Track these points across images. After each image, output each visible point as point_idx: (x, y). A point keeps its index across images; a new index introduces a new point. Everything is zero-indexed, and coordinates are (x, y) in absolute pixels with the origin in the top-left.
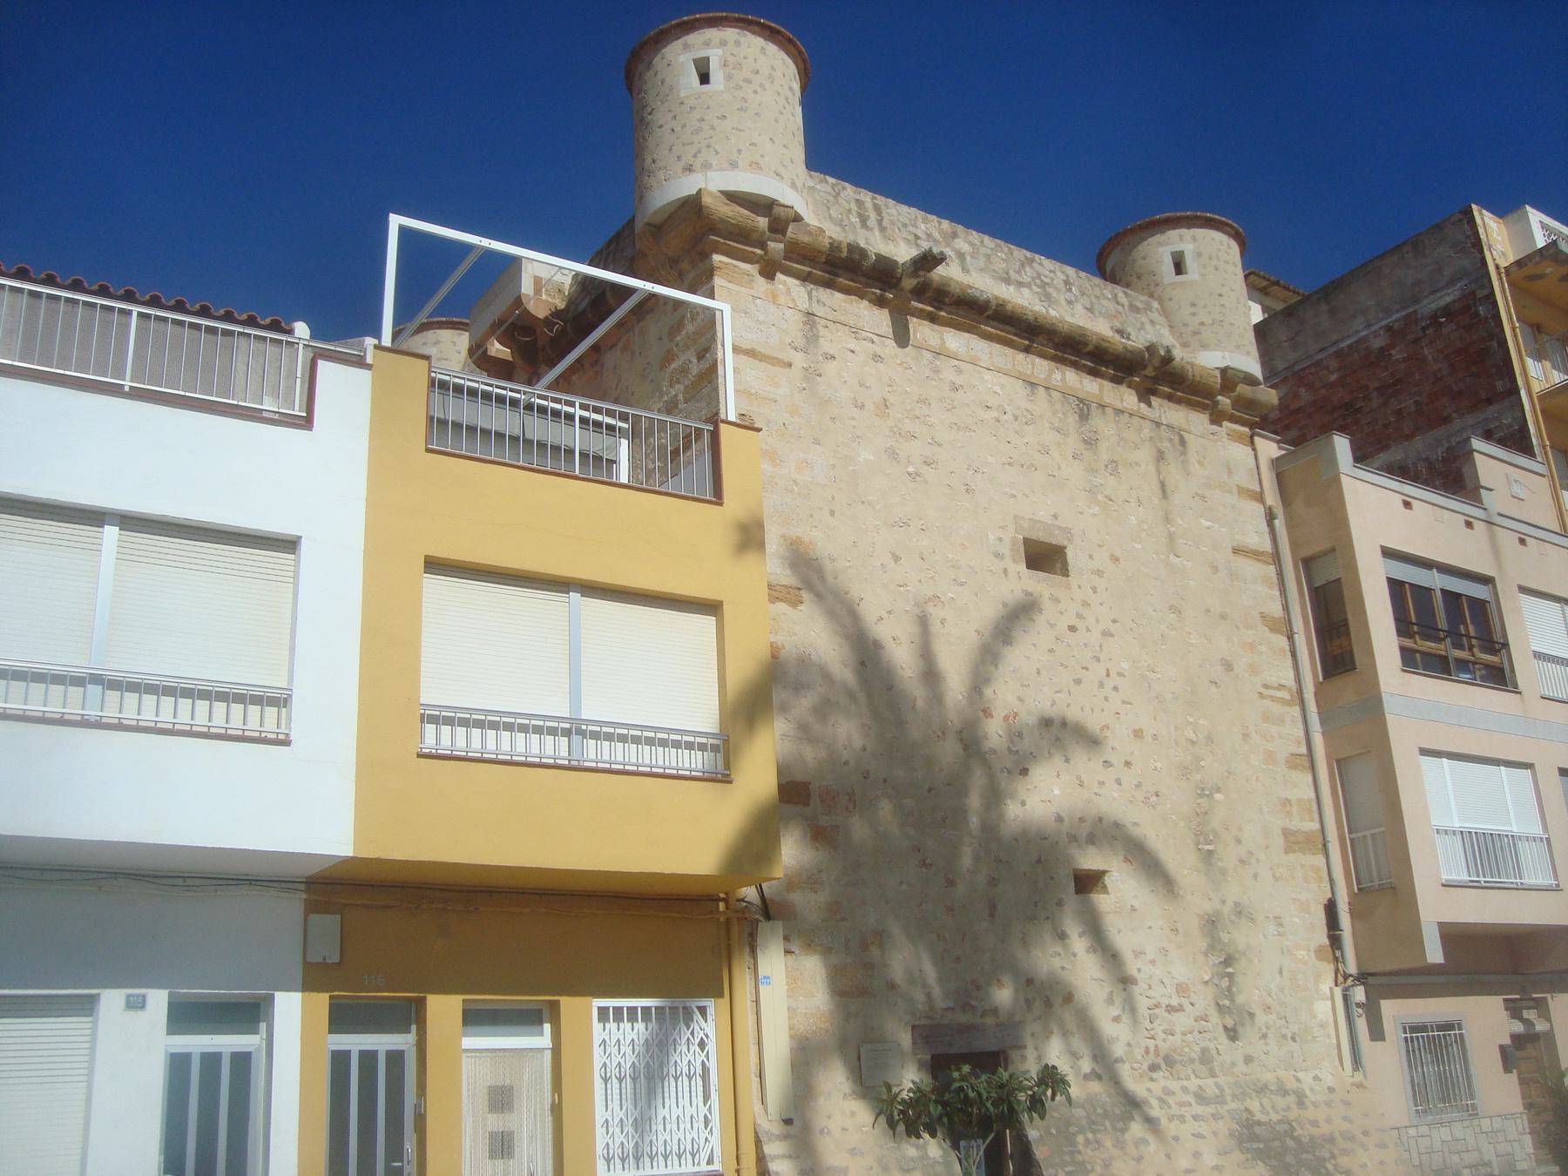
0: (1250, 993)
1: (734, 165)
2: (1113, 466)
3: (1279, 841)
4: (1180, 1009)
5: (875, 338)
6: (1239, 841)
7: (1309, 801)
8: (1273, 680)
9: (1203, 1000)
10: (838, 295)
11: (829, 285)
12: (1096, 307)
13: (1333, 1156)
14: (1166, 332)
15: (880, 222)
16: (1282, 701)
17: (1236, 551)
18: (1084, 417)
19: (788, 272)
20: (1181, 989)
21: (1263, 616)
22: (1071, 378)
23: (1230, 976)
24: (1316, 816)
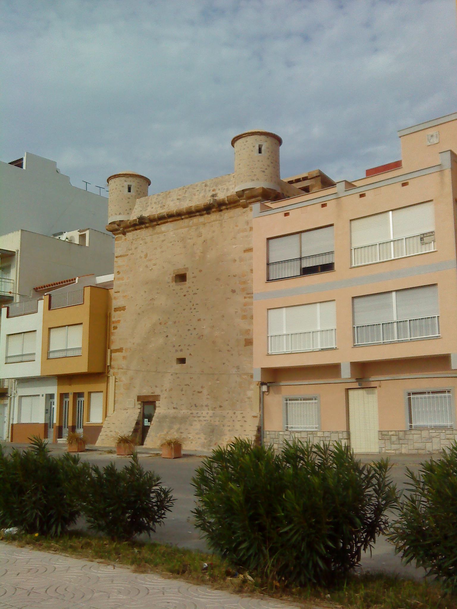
17: (245, 251)
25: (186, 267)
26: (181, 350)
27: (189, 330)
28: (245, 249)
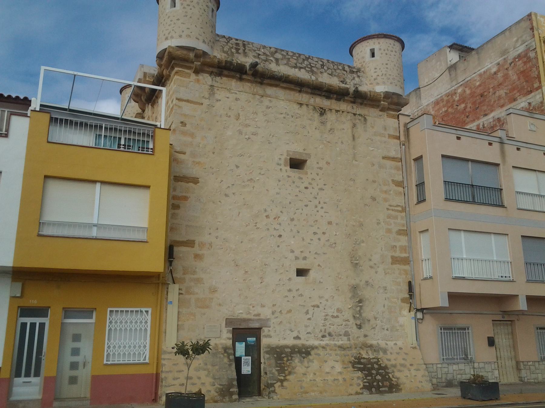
0: (367, 313)
4: (337, 317)
5: (237, 92)
6: (370, 260)
7: (405, 246)
8: (394, 203)
9: (348, 314)
12: (334, 73)
13: (393, 372)
15: (244, 50)
16: (398, 211)
17: (384, 158)
18: (322, 114)
20: (338, 310)
21: (393, 181)
23: (361, 307)
27: (315, 233)
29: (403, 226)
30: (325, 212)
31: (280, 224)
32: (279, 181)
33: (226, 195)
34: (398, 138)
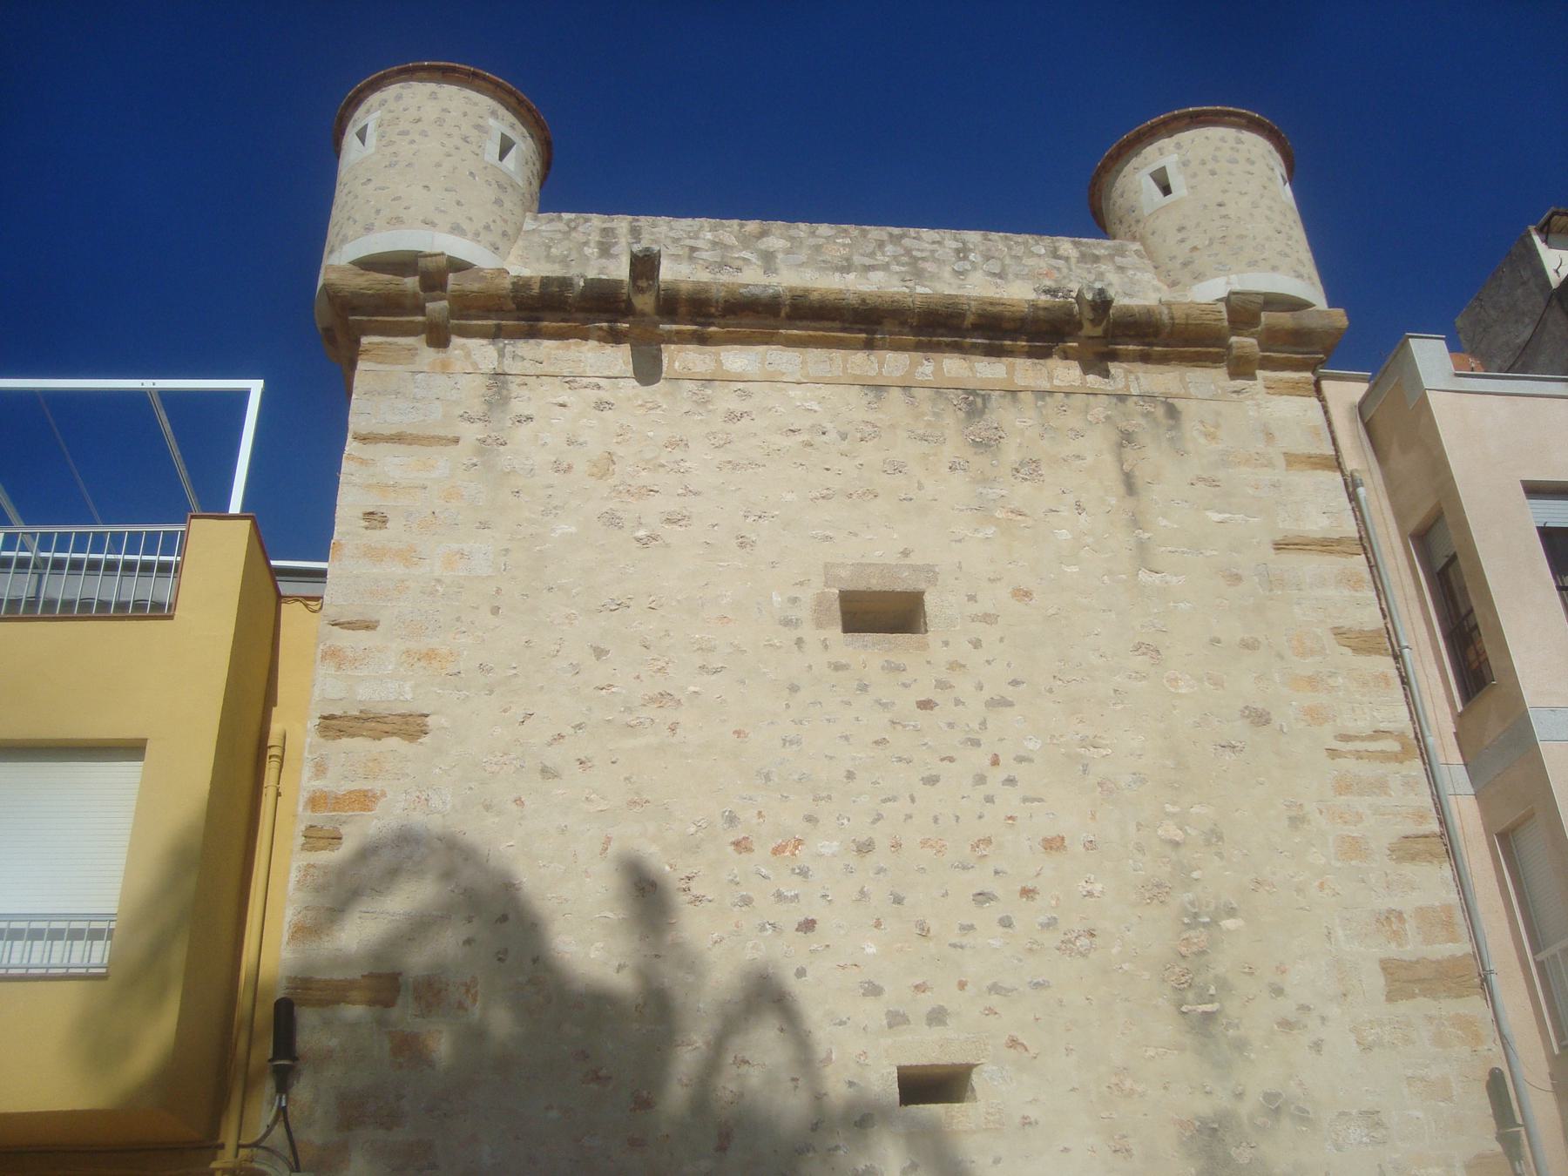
1: (369, 229)
2: (1029, 468)
3: (1376, 982)
5: (602, 382)
6: (1278, 991)
7: (1447, 909)
8: (1363, 725)
10: (547, 343)
11: (532, 334)
14: (1148, 277)
16: (1386, 756)
17: (1280, 546)
19: (466, 333)
21: (1339, 633)
22: (954, 366)
24: (1462, 929)
25: (915, 559)
26: (937, 1017)
27: (982, 897)
28: (1278, 538)
29: (1421, 817)
30: (1025, 800)
31: (804, 873)
32: (794, 689)
33: (547, 772)
34: (1337, 463)
